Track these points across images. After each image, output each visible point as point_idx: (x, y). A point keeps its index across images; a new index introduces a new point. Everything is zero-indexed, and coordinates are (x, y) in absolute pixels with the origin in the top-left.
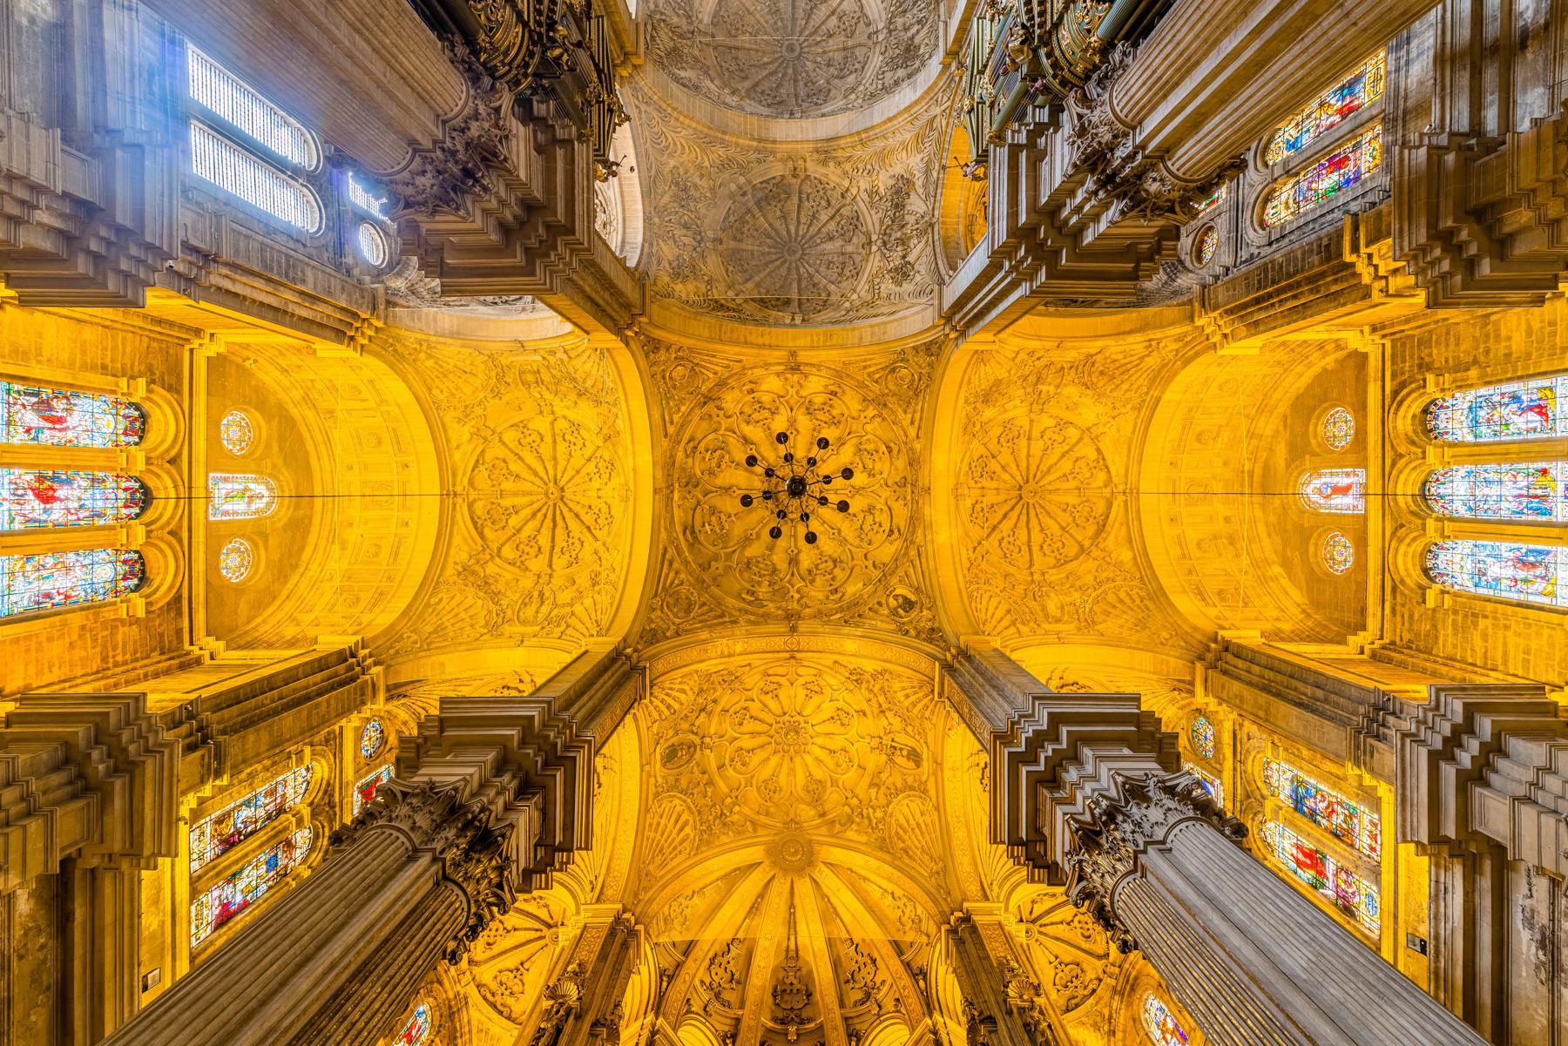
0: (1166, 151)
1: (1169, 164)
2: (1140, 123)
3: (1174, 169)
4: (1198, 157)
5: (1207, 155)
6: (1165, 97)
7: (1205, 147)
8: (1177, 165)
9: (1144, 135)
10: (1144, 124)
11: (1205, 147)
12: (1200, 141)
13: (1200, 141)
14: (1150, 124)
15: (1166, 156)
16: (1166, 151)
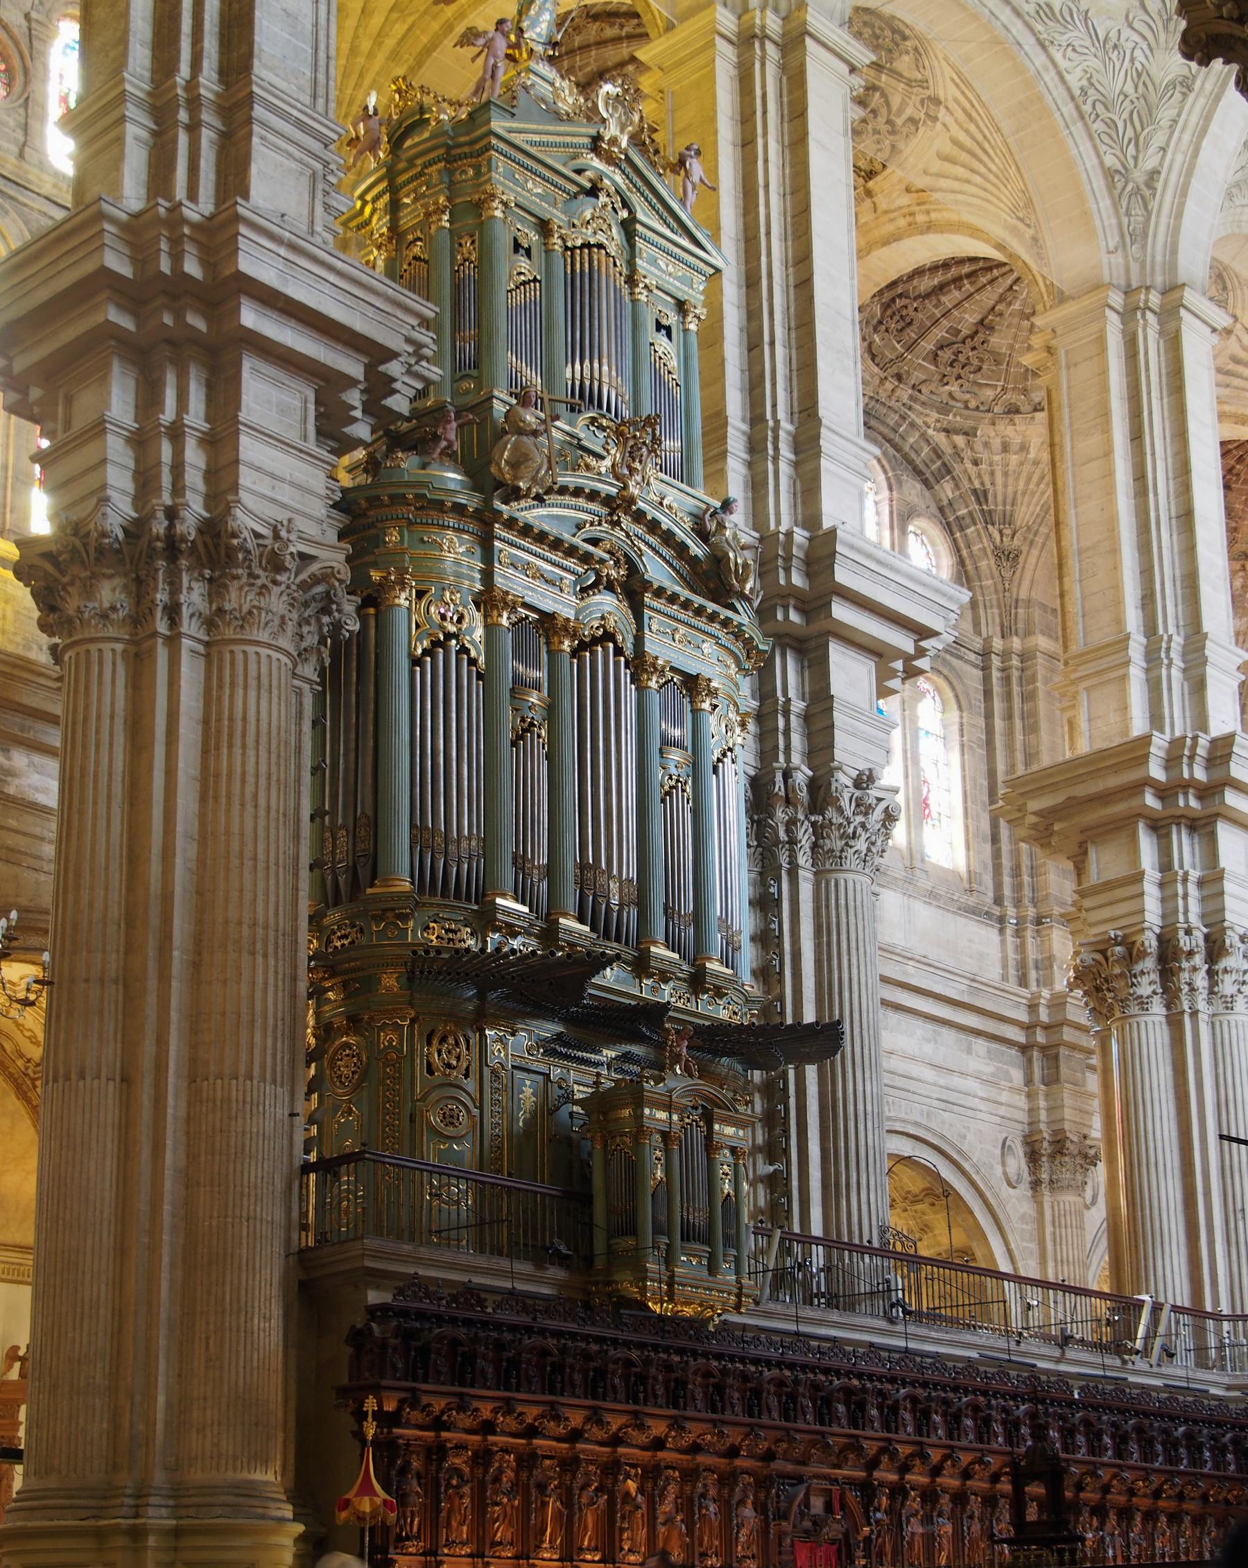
0: (139, 660)
1: (119, 647)
2: (208, 657)
3: (107, 647)
4: (94, 698)
5: (87, 707)
6: (206, 722)
7: (99, 717)
8: (108, 656)
9: (185, 656)
10: (201, 662)
11: (99, 717)
12: (112, 718)
13: (112, 718)
14: (191, 672)
15: (132, 649)
16: (139, 660)
